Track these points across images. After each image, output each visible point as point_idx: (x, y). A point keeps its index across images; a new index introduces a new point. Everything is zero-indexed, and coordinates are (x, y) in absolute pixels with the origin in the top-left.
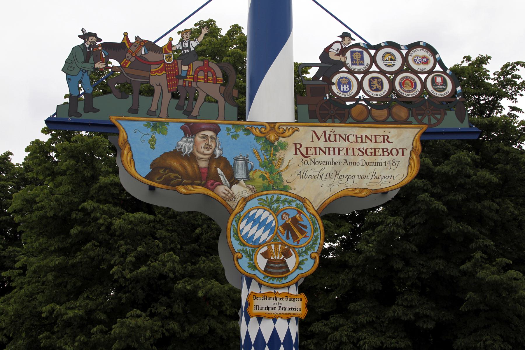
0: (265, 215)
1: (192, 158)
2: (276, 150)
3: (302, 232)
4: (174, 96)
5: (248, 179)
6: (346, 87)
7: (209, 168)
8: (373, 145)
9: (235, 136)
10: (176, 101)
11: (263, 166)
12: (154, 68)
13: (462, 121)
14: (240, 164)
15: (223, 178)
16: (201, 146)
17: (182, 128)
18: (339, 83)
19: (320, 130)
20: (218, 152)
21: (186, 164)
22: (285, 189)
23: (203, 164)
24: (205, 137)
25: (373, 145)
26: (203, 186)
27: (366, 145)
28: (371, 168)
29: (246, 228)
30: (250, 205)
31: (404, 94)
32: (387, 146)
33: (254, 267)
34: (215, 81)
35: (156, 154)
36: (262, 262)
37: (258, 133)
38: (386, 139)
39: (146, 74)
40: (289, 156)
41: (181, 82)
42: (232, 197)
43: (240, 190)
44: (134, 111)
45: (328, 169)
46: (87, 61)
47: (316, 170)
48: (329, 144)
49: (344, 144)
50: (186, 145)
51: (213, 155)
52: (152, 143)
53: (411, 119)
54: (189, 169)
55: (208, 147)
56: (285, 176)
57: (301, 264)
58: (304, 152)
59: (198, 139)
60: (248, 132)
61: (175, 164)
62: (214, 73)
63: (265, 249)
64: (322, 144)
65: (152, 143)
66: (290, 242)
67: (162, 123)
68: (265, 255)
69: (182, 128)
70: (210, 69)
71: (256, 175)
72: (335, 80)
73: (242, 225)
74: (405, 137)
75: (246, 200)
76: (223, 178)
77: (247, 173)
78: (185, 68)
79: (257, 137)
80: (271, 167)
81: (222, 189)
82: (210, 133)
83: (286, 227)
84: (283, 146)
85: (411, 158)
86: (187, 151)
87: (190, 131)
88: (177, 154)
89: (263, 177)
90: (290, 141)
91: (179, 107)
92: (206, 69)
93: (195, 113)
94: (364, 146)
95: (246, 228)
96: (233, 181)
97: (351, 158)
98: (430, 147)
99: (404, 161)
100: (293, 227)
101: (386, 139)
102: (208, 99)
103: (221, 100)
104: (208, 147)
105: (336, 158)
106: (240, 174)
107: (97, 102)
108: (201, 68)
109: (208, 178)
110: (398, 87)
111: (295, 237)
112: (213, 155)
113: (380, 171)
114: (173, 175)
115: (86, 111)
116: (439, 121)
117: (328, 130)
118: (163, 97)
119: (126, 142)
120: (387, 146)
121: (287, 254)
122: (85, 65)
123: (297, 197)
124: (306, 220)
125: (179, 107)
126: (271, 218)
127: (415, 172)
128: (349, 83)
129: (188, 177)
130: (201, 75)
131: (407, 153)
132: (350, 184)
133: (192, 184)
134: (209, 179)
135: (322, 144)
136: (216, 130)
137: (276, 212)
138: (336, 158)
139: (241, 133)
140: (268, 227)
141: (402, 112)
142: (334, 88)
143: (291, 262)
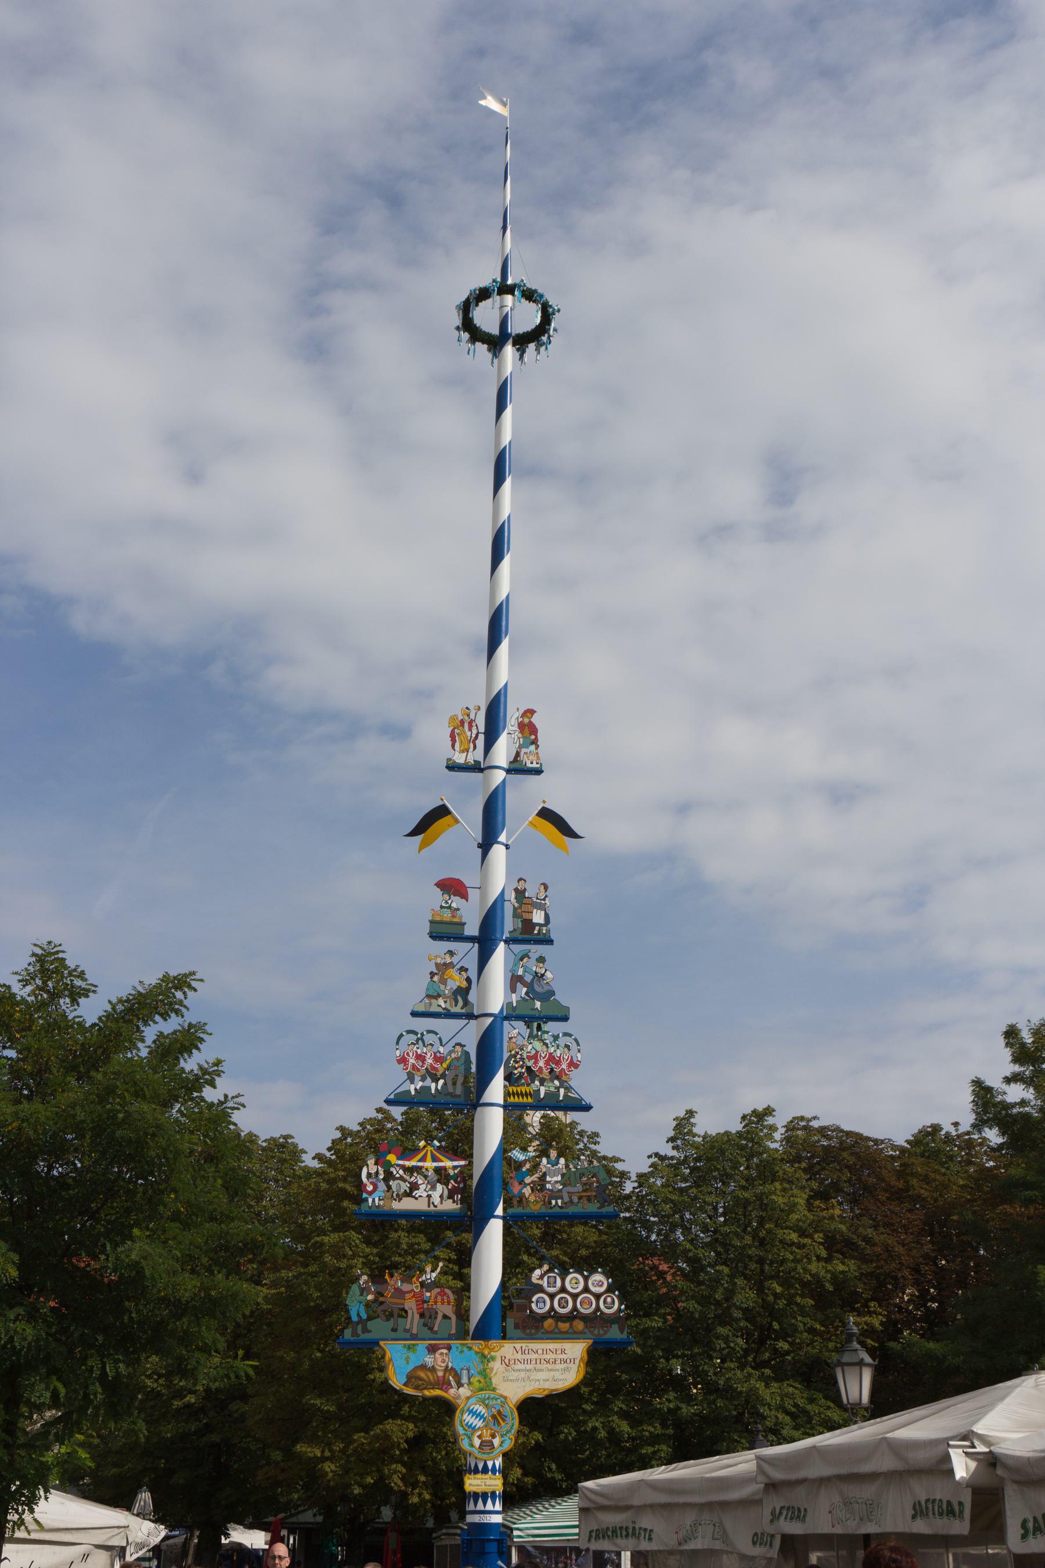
0: (481, 1409)
1: (433, 1369)
2: (489, 1361)
3: (504, 1420)
4: (422, 1315)
5: (470, 1383)
6: (541, 1305)
7: (444, 1377)
8: (554, 1356)
9: (461, 1352)
10: (422, 1320)
11: (480, 1373)
12: (408, 1296)
13: (622, 1332)
14: (465, 1372)
15: (453, 1383)
16: (439, 1361)
17: (427, 1348)
18: (537, 1302)
19: (518, 1346)
20: (450, 1365)
21: (429, 1374)
22: (494, 1390)
23: (440, 1374)
24: (442, 1354)
25: (554, 1356)
26: (441, 1389)
27: (550, 1356)
28: (552, 1373)
29: (468, 1418)
30: (471, 1401)
31: (582, 1311)
32: (564, 1356)
33: (472, 1445)
34: (449, 1303)
35: (410, 1367)
36: (477, 1442)
37: (476, 1349)
38: (563, 1351)
39: (402, 1301)
40: (497, 1365)
41: (425, 1306)
42: (459, 1397)
43: (464, 1392)
44: (394, 1330)
45: (523, 1374)
46: (362, 1294)
47: (513, 1375)
48: (524, 1356)
49: (533, 1356)
50: (429, 1360)
51: (447, 1366)
52: (407, 1360)
53: (586, 1330)
54: (431, 1378)
55: (443, 1361)
56: (494, 1381)
57: (503, 1442)
58: (507, 1361)
59: (437, 1355)
60: (470, 1348)
61: (422, 1374)
62: (448, 1297)
63: (479, 1433)
64: (519, 1356)
65: (407, 1360)
66: (496, 1428)
67: (414, 1345)
68: (479, 1437)
69: (427, 1348)
70: (445, 1294)
71: (474, 1380)
72: (534, 1299)
73: (465, 1416)
74: (576, 1350)
75: (468, 1398)
76: (453, 1383)
77: (469, 1379)
78: (428, 1294)
79: (477, 1353)
80: (485, 1374)
81: (452, 1391)
82: (445, 1351)
83: (494, 1417)
84: (493, 1359)
85: (579, 1366)
86: (430, 1365)
87: (432, 1350)
88: (423, 1367)
89: (480, 1382)
90: (498, 1355)
91: (425, 1325)
92: (442, 1294)
93: (436, 1328)
94: (547, 1357)
95: (468, 1418)
96: (460, 1385)
97: (538, 1366)
98: (593, 1356)
99: (574, 1368)
100: (498, 1418)
101: (563, 1351)
102: (445, 1317)
103: (454, 1318)
104: (443, 1361)
105: (529, 1367)
106: (464, 1380)
107: (370, 1325)
108: (439, 1293)
109: (443, 1384)
110: (578, 1305)
111: (499, 1424)
112: (447, 1366)
113: (558, 1375)
114: (420, 1383)
115: (363, 1332)
116: (606, 1333)
117: (524, 1345)
118: (413, 1321)
119: (391, 1360)
120: (564, 1356)
121: (493, 1436)
122: (362, 1298)
123: (502, 1396)
124: (506, 1411)
125: (425, 1325)
126: (484, 1411)
127: (581, 1376)
128: (544, 1302)
129: (431, 1383)
130: (439, 1298)
131: (577, 1361)
132: (537, 1385)
133: (433, 1388)
134: (444, 1384)
135: (519, 1356)
136: (449, 1348)
137: (487, 1406)
138: (529, 1367)
139: (465, 1349)
140: (482, 1417)
141: (579, 1325)
142: (533, 1306)
143: (496, 1442)
